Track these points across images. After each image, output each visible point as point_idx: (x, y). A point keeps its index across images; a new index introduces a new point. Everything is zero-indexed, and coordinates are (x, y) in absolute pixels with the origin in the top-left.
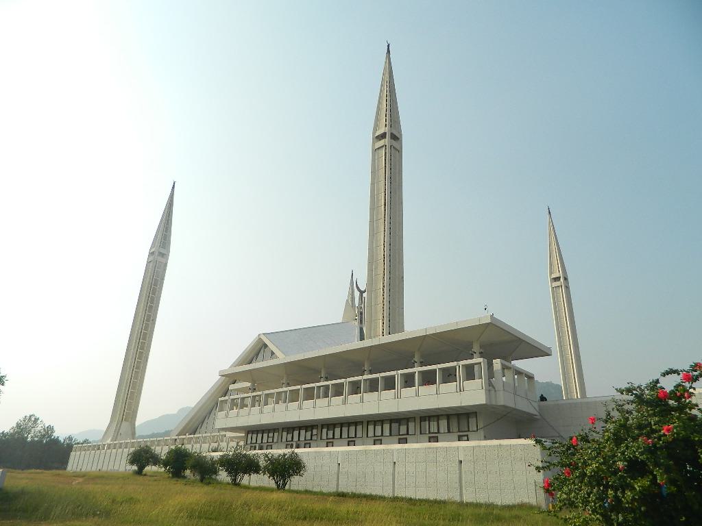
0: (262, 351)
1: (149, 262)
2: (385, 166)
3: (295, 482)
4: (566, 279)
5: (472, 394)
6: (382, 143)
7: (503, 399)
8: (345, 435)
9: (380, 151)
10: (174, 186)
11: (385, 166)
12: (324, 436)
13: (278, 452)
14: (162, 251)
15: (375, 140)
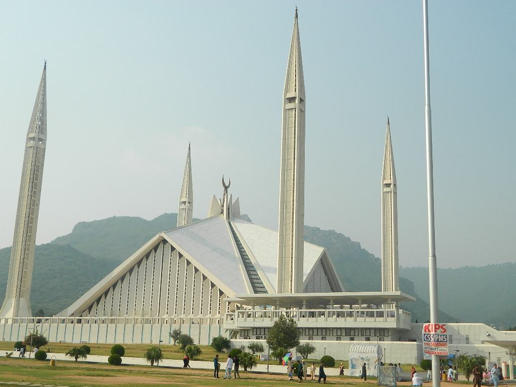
0: (161, 245)
1: (27, 148)
2: (295, 126)
3: (311, 356)
4: (395, 185)
5: (391, 323)
6: (291, 105)
7: (402, 326)
8: (320, 333)
9: (290, 112)
10: (45, 66)
11: (295, 126)
12: (307, 334)
13: (303, 342)
14: (41, 136)
15: (286, 100)
